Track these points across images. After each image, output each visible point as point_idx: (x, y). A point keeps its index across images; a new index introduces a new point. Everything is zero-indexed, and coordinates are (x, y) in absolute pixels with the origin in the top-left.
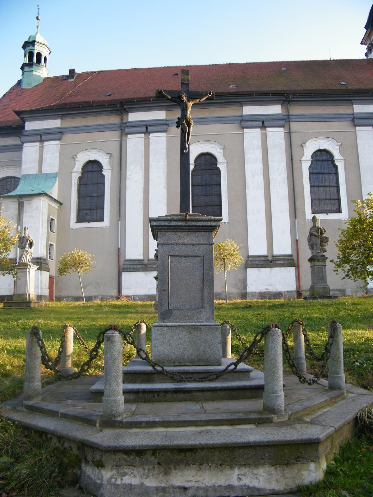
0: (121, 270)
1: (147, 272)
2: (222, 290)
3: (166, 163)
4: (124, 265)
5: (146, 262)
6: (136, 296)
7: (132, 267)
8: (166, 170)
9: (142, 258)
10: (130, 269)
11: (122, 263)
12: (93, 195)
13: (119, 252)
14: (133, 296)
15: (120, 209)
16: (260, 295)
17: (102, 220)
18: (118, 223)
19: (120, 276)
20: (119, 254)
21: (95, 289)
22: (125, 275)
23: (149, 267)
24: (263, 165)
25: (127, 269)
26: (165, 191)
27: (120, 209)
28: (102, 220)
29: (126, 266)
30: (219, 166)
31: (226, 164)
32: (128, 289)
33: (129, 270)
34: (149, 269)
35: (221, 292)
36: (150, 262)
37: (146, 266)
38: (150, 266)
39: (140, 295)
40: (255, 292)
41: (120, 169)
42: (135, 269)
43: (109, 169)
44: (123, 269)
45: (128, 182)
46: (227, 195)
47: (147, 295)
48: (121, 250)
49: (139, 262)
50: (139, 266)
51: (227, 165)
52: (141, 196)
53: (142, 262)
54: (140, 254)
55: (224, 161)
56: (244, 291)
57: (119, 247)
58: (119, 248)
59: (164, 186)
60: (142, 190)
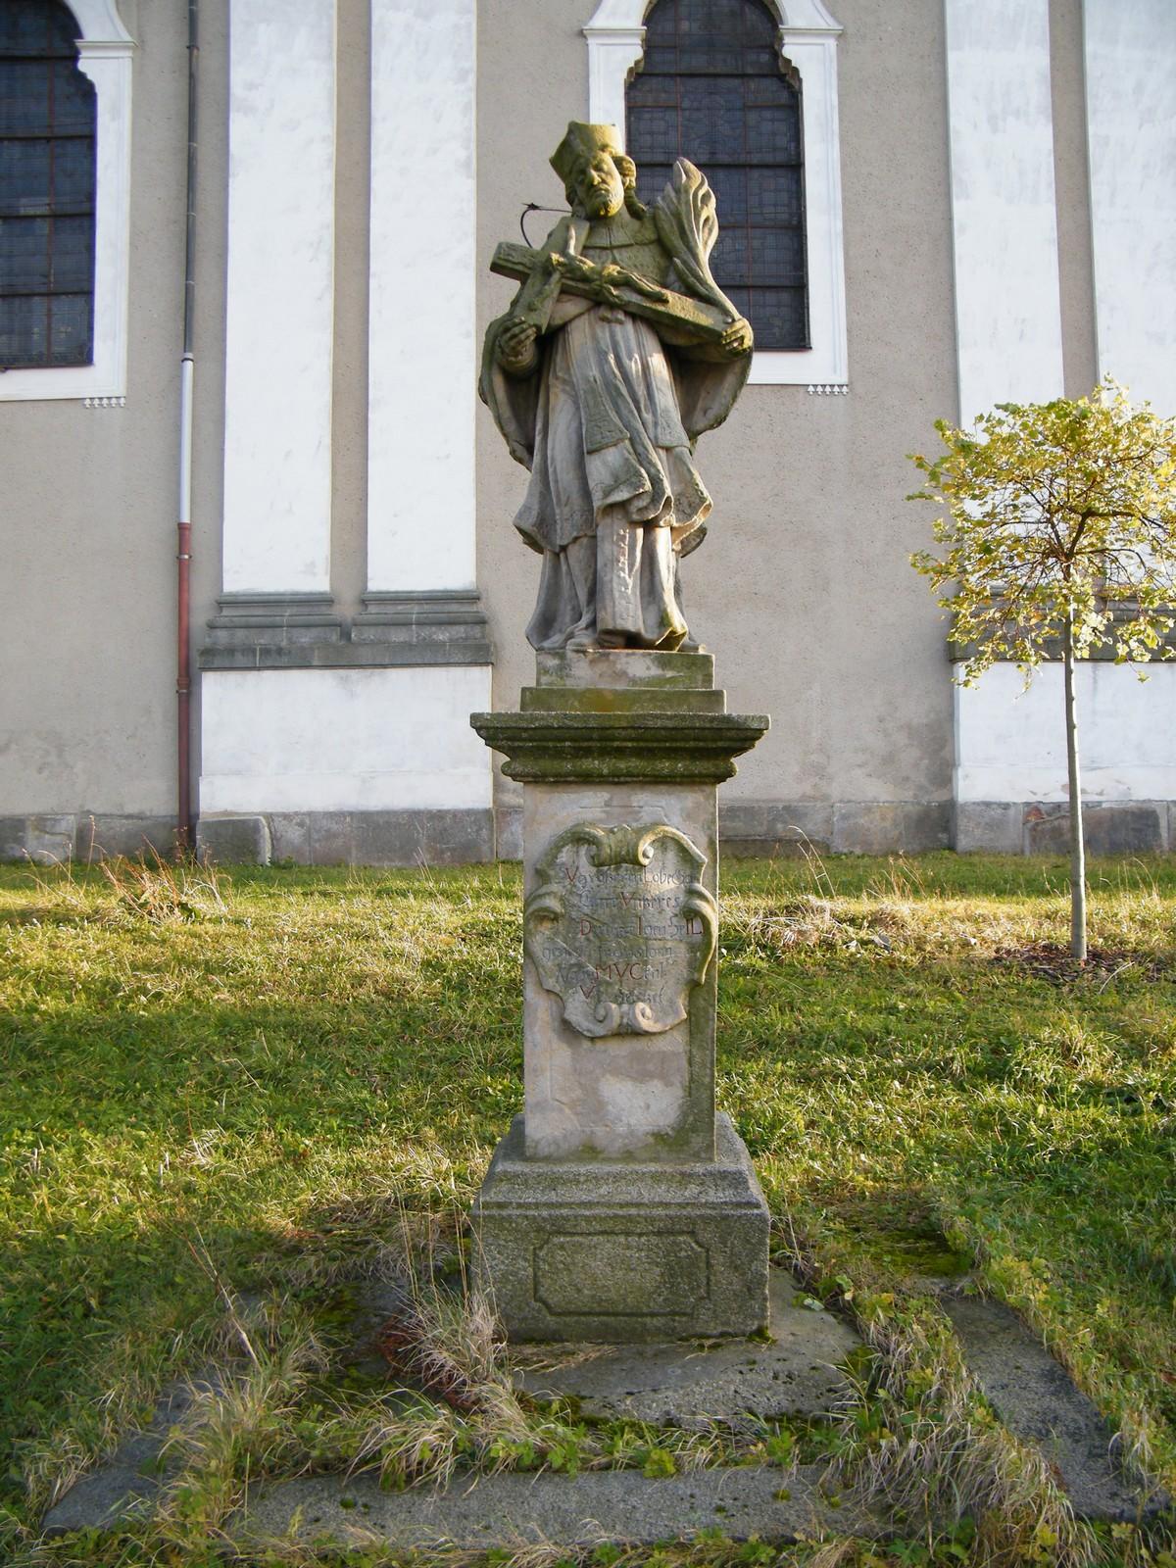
0: (197, 661)
1: (354, 674)
2: (807, 788)
3: (473, 19)
4: (212, 627)
5: (346, 611)
6: (286, 816)
7: (263, 639)
8: (471, 62)
9: (320, 584)
10: (249, 650)
11: (199, 617)
12: (27, 206)
13: (181, 552)
14: (270, 817)
15: (189, 291)
16: (1033, 819)
17: (81, 356)
18: (179, 377)
19: (189, 695)
20: (180, 561)
21: (40, 770)
22: (217, 691)
23: (363, 643)
24: (1053, 58)
25: (231, 651)
26: (470, 185)
27: (189, 291)
28: (81, 356)
29: (222, 636)
30: (791, 50)
31: (831, 44)
32: (238, 773)
33: (240, 660)
34: (365, 655)
35: (804, 798)
36: (373, 609)
37: (346, 635)
38: (370, 634)
39: (310, 814)
40: (1006, 806)
41: (192, 46)
42: (280, 651)
43: (122, 46)
44: (208, 652)
45: (240, 128)
46: (839, 225)
47: (351, 814)
48: (198, 540)
49: (305, 610)
50: (305, 638)
51: (842, 51)
52: (319, 213)
53: (324, 609)
54: (313, 564)
55: (824, 21)
56: (938, 796)
57: (186, 519)
58: (182, 528)
59: (462, 154)
60: (329, 177)
